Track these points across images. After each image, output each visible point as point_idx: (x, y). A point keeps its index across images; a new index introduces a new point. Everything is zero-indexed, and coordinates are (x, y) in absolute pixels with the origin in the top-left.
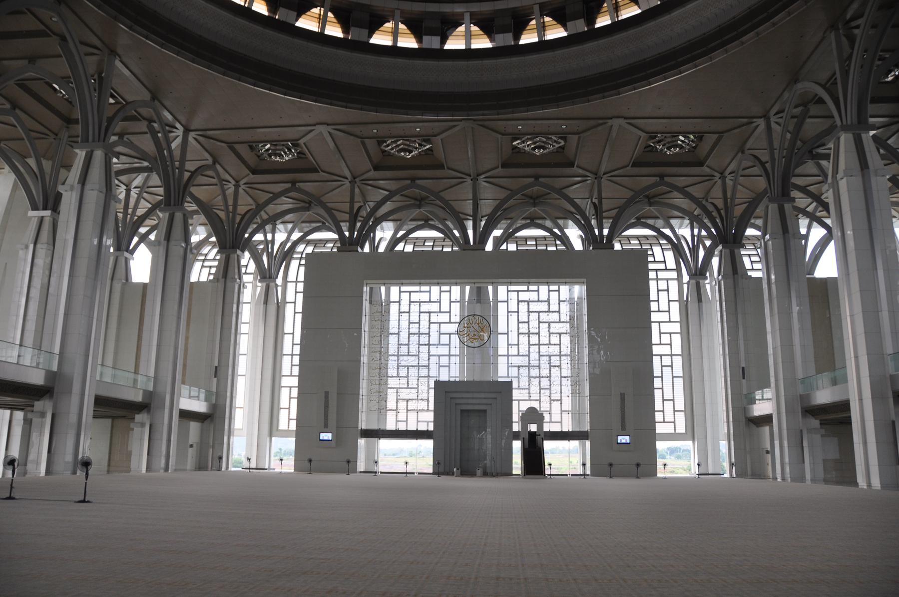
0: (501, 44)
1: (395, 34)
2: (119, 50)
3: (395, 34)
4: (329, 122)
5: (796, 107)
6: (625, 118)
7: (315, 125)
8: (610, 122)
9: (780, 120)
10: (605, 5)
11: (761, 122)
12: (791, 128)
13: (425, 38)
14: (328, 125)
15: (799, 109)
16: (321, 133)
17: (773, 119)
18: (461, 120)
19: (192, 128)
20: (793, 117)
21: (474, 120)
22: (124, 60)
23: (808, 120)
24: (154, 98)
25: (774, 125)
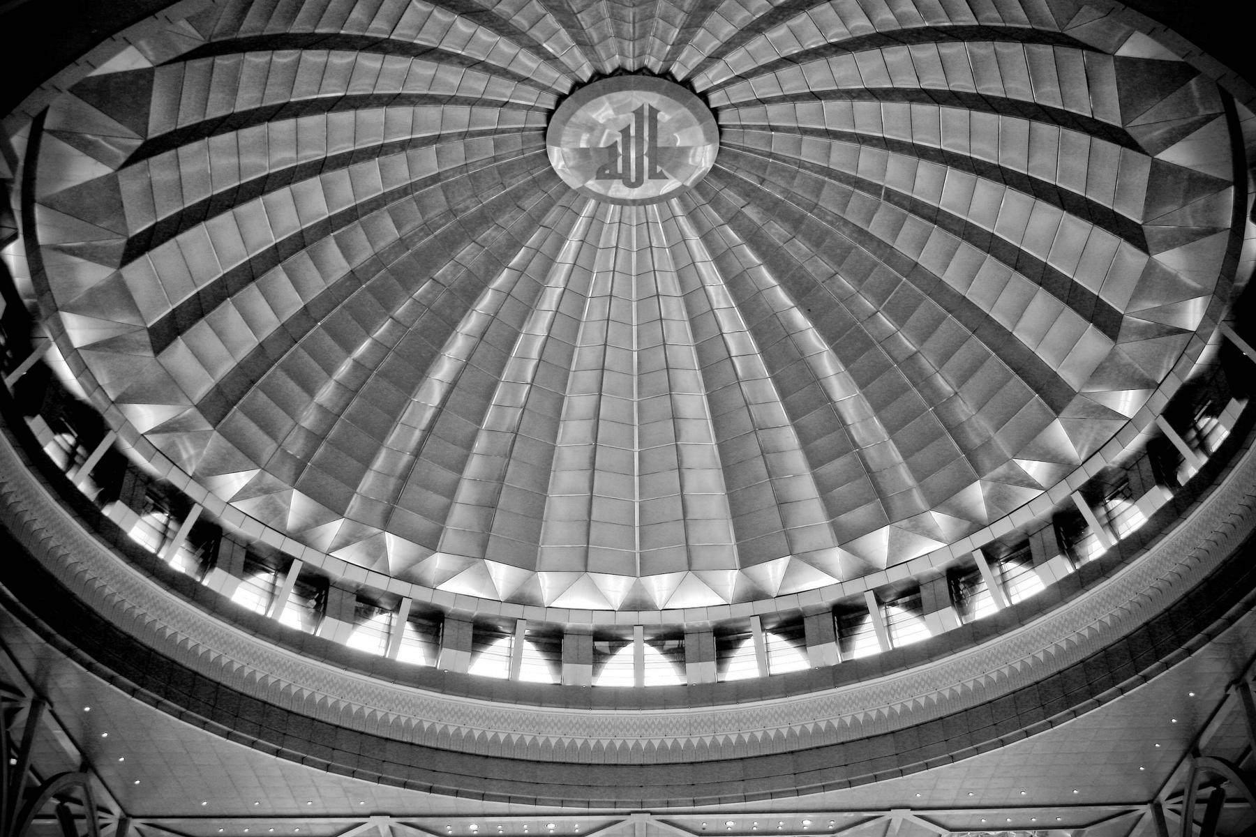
0: (695, 681)
1: (515, 659)
2: (53, 696)
3: (515, 659)
4: (393, 811)
5: (1202, 786)
6: (913, 809)
7: (368, 816)
8: (887, 815)
9: (1179, 807)
10: (869, 619)
11: (1146, 810)
12: (1200, 817)
13: (565, 666)
14: (392, 816)
15: (1210, 790)
16: (376, 827)
17: (1167, 807)
18: (629, 814)
19: (134, 813)
20: (1199, 801)
21: (652, 813)
22: (59, 710)
23: (1226, 806)
24: (87, 765)
25: (1167, 814)
